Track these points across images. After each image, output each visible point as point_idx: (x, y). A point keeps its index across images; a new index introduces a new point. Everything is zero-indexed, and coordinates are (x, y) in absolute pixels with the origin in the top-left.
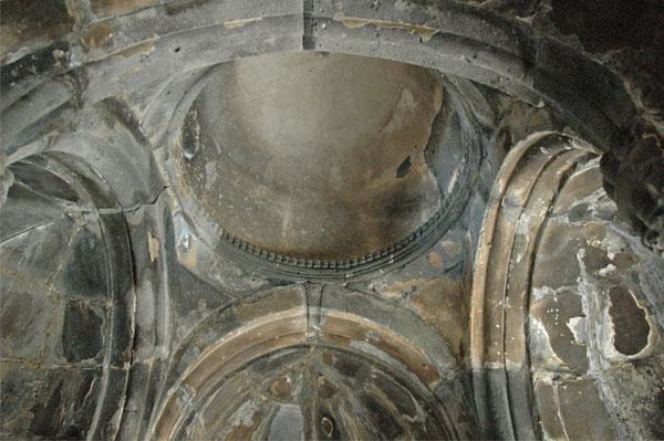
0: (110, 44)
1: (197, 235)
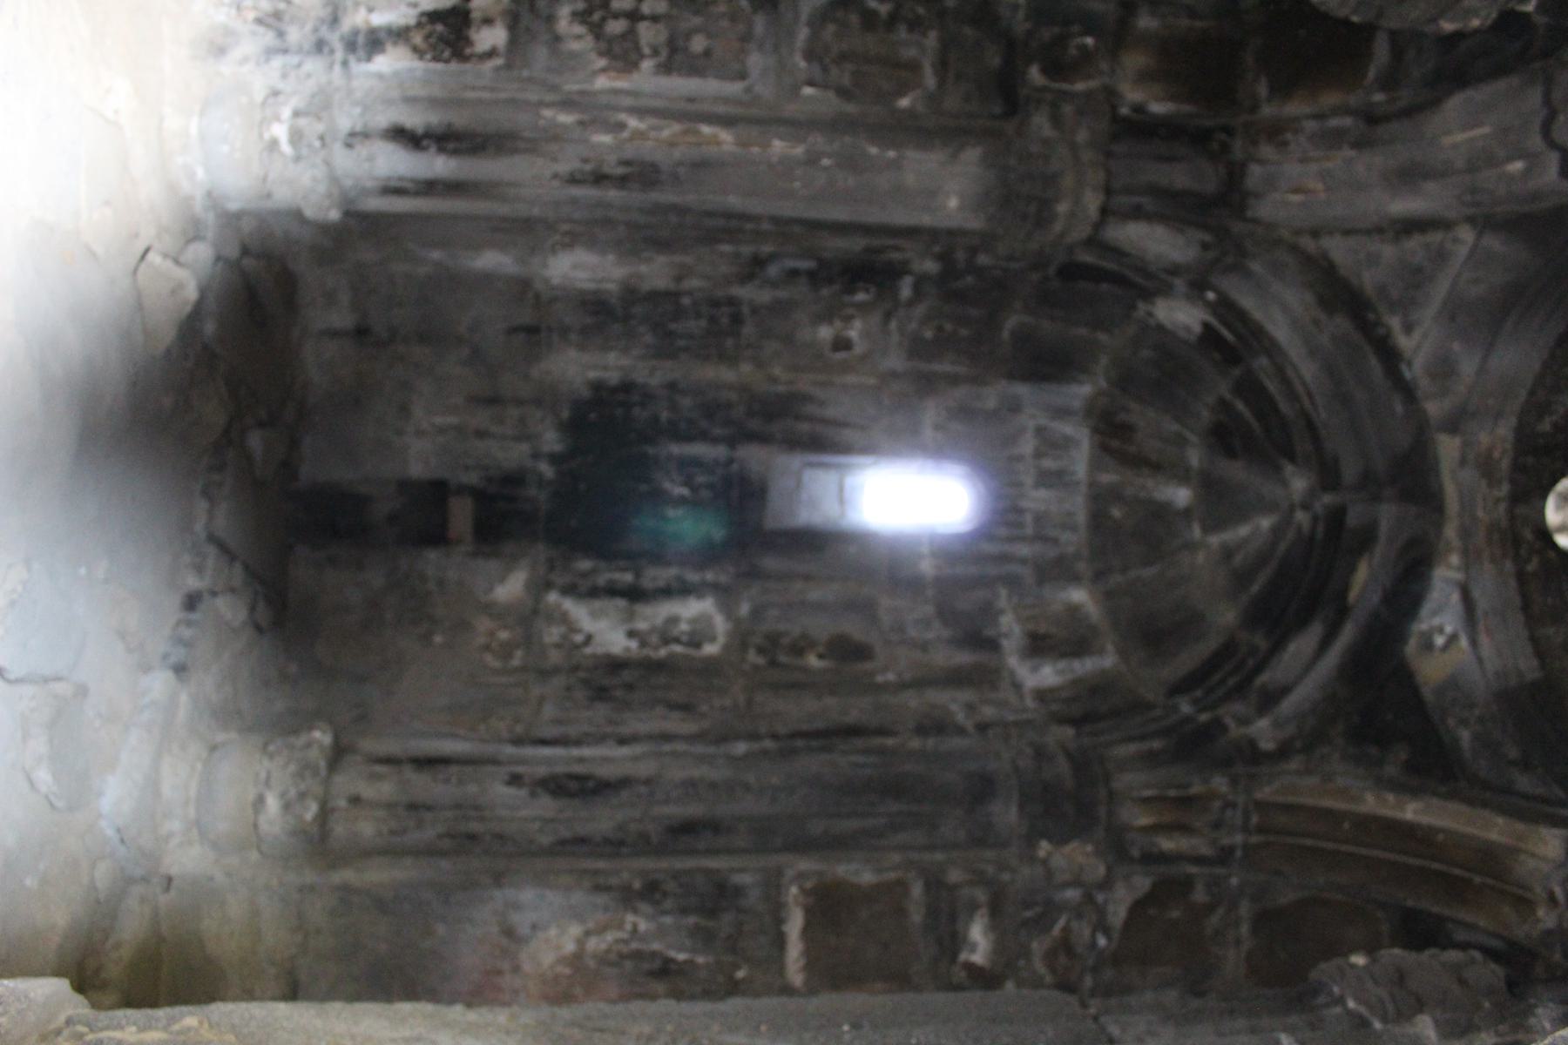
0: (1285, 144)
1: (1474, 643)
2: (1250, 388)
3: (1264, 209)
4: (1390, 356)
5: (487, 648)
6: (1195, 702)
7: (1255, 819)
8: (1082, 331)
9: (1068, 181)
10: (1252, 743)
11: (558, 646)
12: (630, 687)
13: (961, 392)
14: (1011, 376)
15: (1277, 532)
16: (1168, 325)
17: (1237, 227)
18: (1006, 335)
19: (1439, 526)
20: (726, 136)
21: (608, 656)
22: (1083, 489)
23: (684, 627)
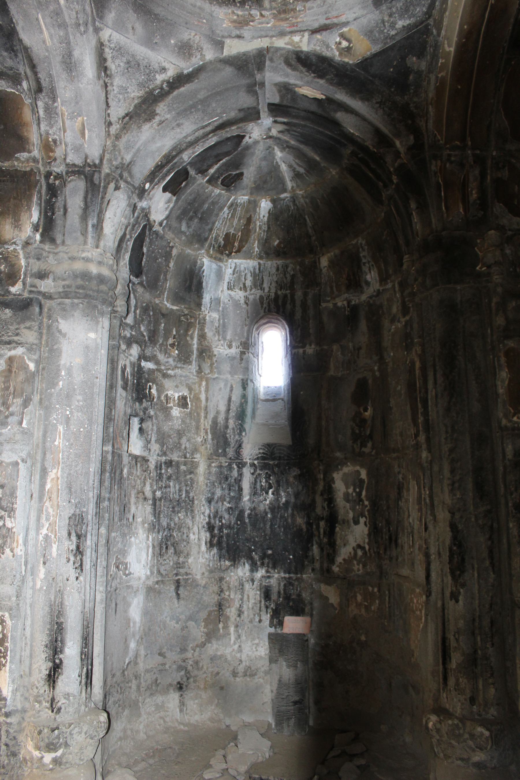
0: (55, 141)
2: (202, 163)
3: (94, 153)
4: (180, 80)
5: (367, 608)
6: (385, 186)
7: (458, 143)
8: (171, 265)
9: (78, 266)
10: (410, 149)
11: (364, 566)
12: (388, 523)
13: (209, 333)
14: (199, 305)
15: (285, 147)
16: (167, 213)
17: (106, 170)
18: (175, 308)
19: (278, 49)
20: (52, 474)
21: (369, 535)
22: (261, 262)
23: (351, 490)
